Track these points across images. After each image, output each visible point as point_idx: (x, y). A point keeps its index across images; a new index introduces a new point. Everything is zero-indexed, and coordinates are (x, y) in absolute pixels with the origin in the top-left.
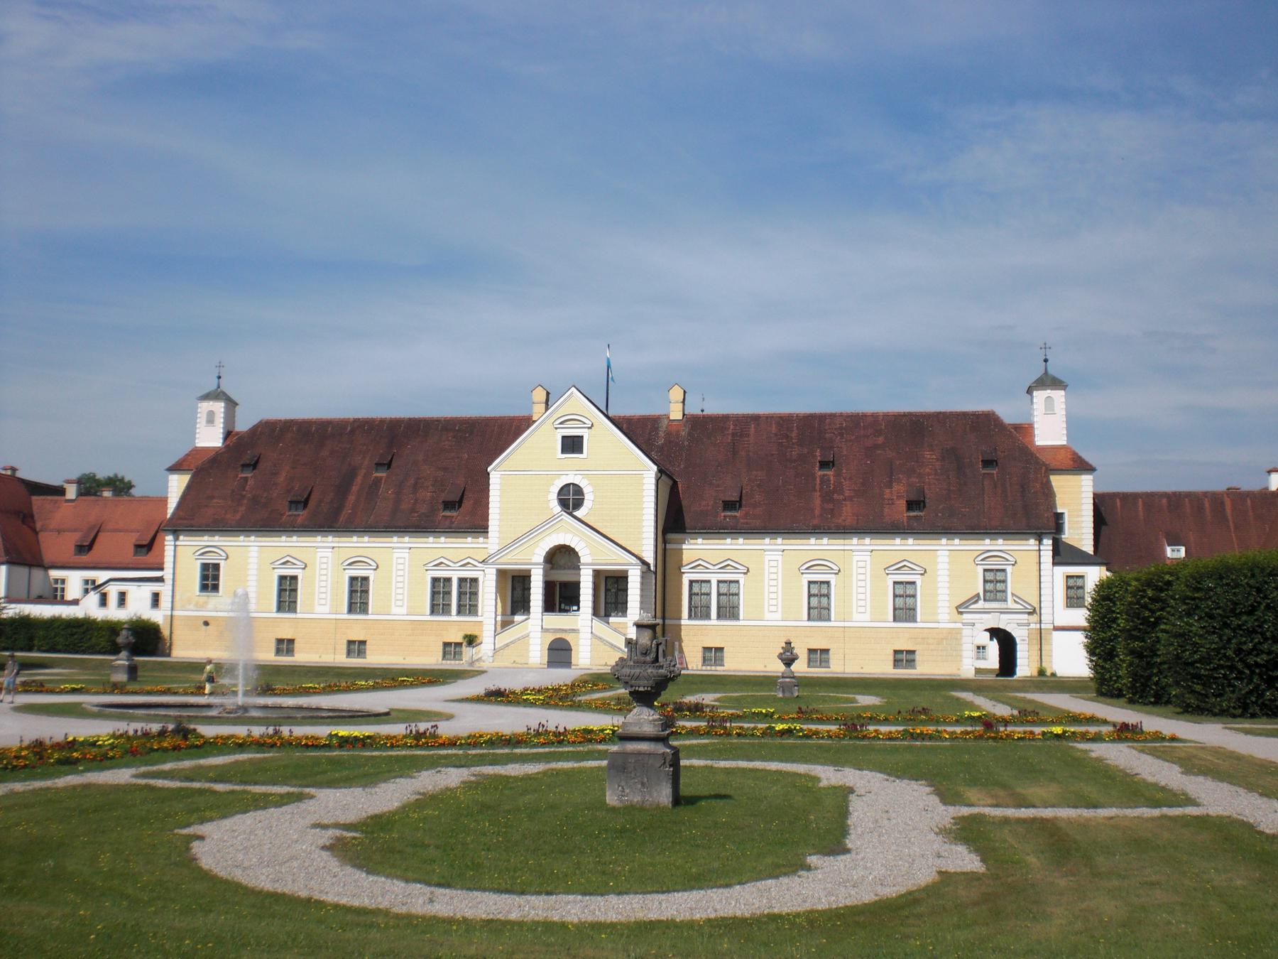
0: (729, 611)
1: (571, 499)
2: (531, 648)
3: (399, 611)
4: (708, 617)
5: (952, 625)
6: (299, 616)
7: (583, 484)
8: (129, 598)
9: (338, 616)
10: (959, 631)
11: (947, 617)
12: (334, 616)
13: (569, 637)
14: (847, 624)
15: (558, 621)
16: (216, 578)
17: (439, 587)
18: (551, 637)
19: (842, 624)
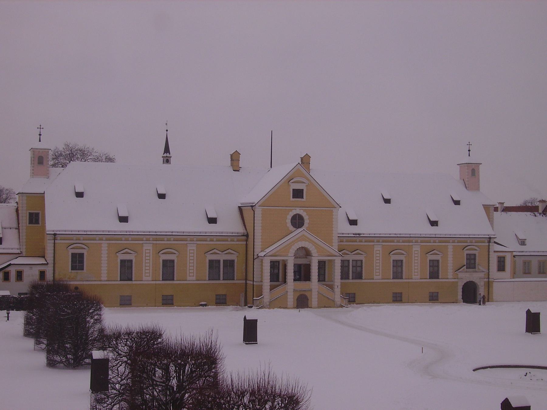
0: (359, 276)
1: (298, 221)
2: (289, 300)
3: (191, 278)
4: (349, 279)
5: (454, 280)
6: (134, 282)
7: (304, 214)
8: (25, 275)
9: (158, 282)
10: (457, 282)
11: (452, 277)
12: (154, 282)
13: (306, 294)
14: (410, 281)
15: (302, 285)
16: (82, 262)
17: (214, 265)
18: (298, 294)
19: (408, 281)
